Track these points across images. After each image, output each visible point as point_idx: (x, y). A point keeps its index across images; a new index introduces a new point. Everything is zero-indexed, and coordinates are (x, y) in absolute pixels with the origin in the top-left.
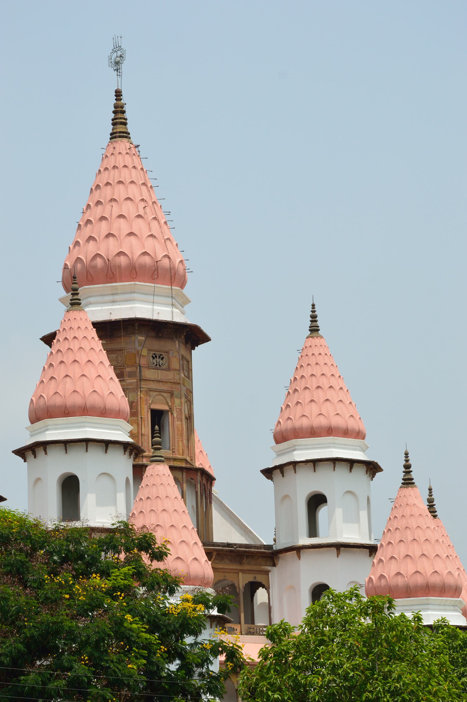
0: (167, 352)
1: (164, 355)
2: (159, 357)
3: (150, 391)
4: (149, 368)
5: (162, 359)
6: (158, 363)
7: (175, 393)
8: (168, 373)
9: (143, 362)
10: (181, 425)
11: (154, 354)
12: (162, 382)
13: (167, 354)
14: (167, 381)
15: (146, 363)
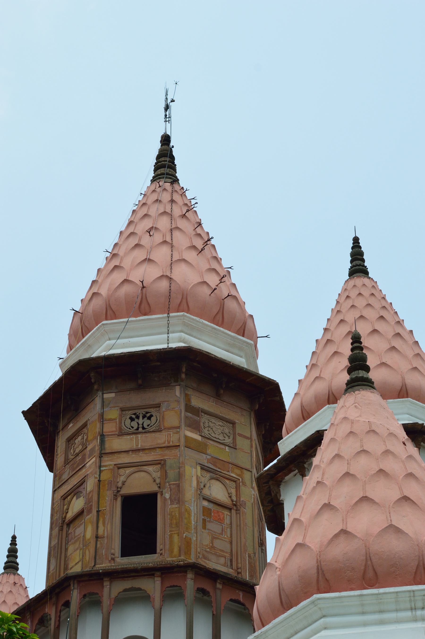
0: (158, 406)
1: (153, 411)
2: (144, 417)
3: (119, 468)
4: (121, 434)
5: (149, 418)
6: (141, 426)
7: (168, 462)
8: (157, 435)
9: (109, 428)
10: (177, 509)
11: (135, 414)
12: (143, 450)
13: (157, 409)
14: (152, 447)
15: (114, 429)
